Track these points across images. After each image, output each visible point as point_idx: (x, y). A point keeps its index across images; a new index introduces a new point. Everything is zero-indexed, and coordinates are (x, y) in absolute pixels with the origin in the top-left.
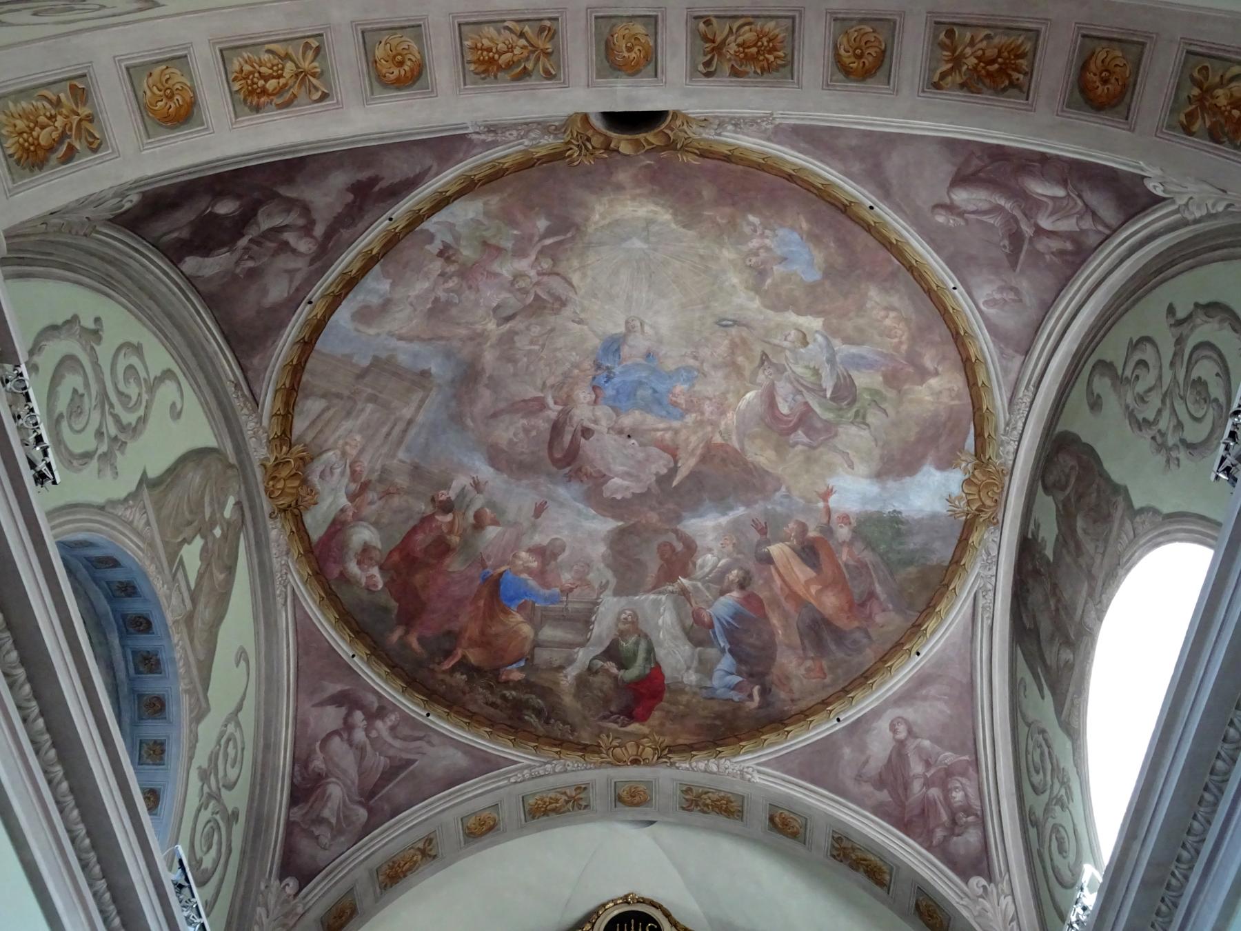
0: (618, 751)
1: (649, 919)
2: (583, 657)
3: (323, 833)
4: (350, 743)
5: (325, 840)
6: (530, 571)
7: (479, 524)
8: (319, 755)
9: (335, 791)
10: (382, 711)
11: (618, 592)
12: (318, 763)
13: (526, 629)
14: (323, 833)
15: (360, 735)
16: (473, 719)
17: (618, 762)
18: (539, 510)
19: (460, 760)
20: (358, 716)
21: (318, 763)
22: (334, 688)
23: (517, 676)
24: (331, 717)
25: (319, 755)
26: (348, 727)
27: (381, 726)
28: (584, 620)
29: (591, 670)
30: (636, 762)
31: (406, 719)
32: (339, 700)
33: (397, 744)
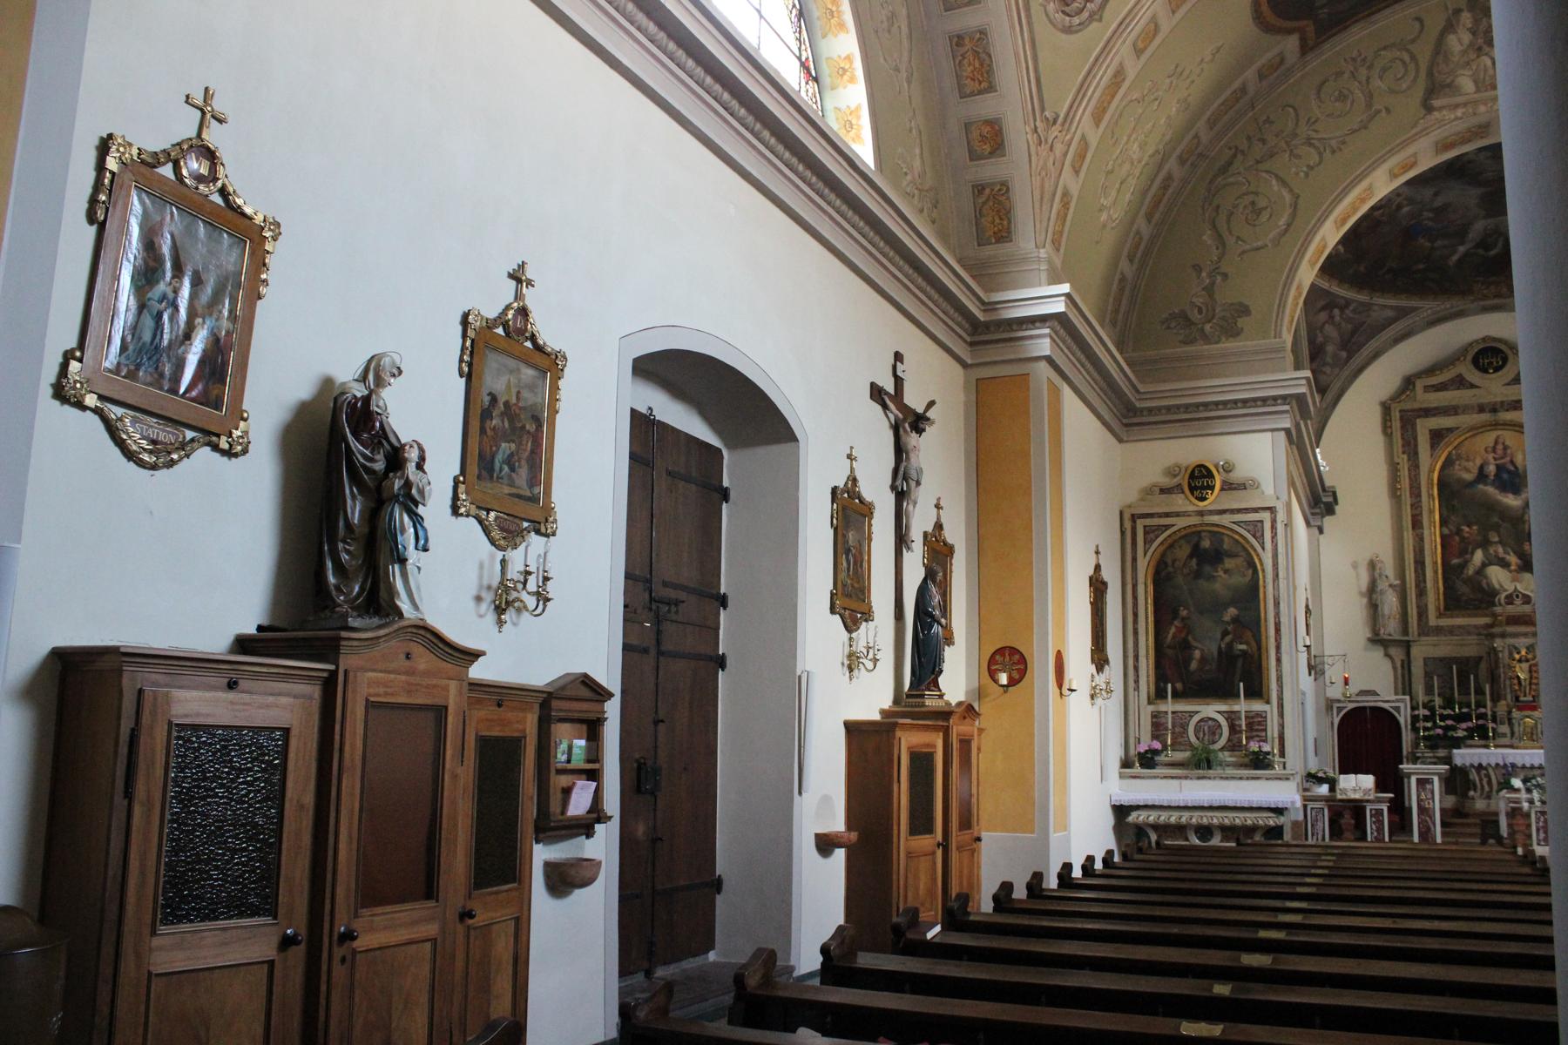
0: (1485, 292)
1: (1499, 351)
2: (1462, 249)
3: (1328, 370)
4: (1333, 324)
5: (1328, 372)
6: (1429, 219)
7: (1399, 207)
8: (1320, 335)
9: (1330, 348)
10: (1348, 302)
11: (1485, 217)
12: (1320, 339)
13: (1428, 244)
14: (1328, 370)
15: (1337, 319)
16: (1397, 291)
17: (1485, 297)
18: (1436, 194)
19: (1390, 313)
20: (1336, 312)
21: (1320, 339)
22: (1322, 303)
23: (1421, 266)
24: (1323, 316)
25: (1320, 335)
26: (1332, 317)
27: (1347, 311)
28: (1461, 234)
29: (1466, 255)
30: (1495, 297)
31: (1362, 304)
32: (1323, 308)
33: (1356, 316)
